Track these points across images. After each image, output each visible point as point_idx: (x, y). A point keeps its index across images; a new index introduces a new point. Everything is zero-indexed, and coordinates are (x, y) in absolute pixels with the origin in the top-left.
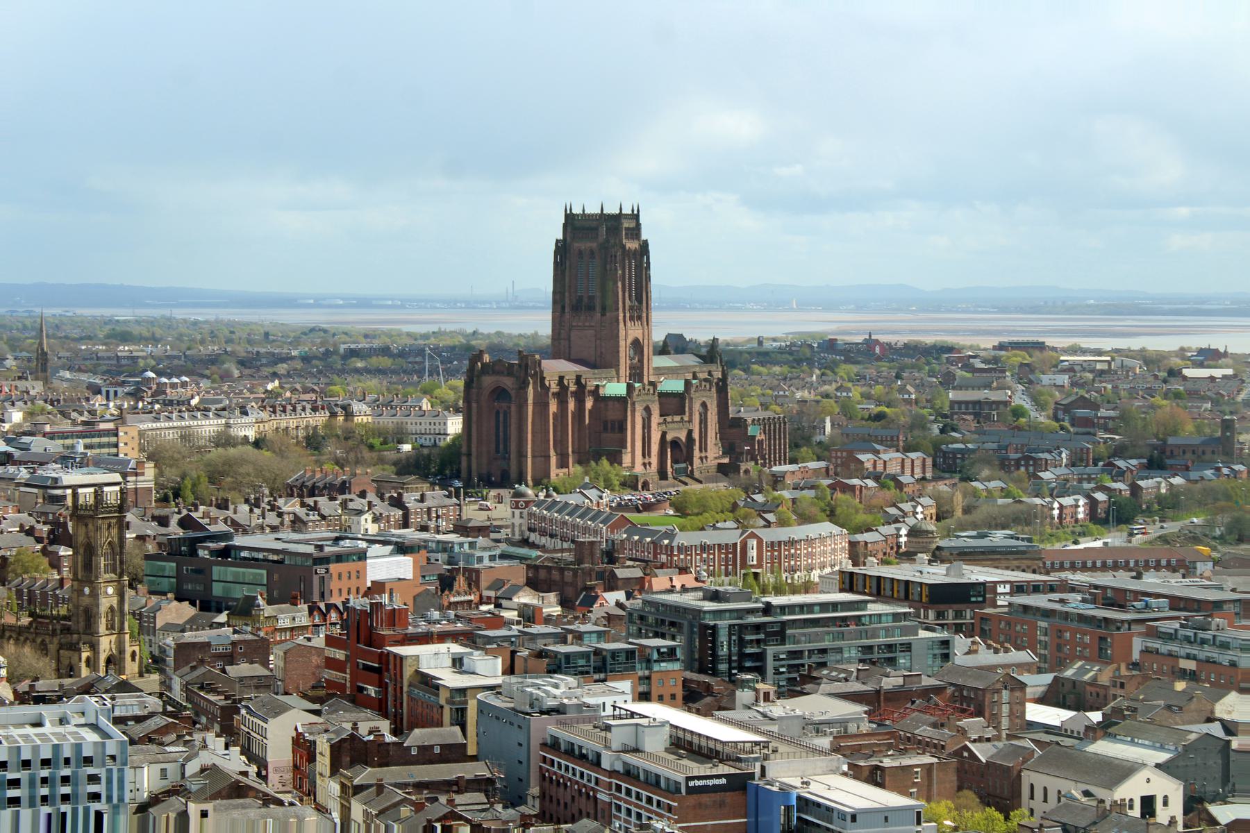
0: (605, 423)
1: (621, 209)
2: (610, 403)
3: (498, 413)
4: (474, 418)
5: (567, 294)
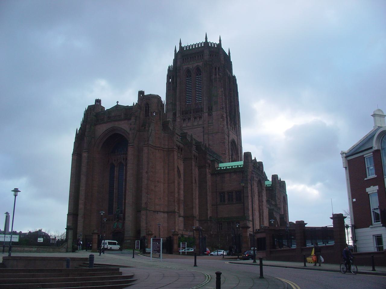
1: (220, 41)
4: (84, 169)
5: (178, 103)
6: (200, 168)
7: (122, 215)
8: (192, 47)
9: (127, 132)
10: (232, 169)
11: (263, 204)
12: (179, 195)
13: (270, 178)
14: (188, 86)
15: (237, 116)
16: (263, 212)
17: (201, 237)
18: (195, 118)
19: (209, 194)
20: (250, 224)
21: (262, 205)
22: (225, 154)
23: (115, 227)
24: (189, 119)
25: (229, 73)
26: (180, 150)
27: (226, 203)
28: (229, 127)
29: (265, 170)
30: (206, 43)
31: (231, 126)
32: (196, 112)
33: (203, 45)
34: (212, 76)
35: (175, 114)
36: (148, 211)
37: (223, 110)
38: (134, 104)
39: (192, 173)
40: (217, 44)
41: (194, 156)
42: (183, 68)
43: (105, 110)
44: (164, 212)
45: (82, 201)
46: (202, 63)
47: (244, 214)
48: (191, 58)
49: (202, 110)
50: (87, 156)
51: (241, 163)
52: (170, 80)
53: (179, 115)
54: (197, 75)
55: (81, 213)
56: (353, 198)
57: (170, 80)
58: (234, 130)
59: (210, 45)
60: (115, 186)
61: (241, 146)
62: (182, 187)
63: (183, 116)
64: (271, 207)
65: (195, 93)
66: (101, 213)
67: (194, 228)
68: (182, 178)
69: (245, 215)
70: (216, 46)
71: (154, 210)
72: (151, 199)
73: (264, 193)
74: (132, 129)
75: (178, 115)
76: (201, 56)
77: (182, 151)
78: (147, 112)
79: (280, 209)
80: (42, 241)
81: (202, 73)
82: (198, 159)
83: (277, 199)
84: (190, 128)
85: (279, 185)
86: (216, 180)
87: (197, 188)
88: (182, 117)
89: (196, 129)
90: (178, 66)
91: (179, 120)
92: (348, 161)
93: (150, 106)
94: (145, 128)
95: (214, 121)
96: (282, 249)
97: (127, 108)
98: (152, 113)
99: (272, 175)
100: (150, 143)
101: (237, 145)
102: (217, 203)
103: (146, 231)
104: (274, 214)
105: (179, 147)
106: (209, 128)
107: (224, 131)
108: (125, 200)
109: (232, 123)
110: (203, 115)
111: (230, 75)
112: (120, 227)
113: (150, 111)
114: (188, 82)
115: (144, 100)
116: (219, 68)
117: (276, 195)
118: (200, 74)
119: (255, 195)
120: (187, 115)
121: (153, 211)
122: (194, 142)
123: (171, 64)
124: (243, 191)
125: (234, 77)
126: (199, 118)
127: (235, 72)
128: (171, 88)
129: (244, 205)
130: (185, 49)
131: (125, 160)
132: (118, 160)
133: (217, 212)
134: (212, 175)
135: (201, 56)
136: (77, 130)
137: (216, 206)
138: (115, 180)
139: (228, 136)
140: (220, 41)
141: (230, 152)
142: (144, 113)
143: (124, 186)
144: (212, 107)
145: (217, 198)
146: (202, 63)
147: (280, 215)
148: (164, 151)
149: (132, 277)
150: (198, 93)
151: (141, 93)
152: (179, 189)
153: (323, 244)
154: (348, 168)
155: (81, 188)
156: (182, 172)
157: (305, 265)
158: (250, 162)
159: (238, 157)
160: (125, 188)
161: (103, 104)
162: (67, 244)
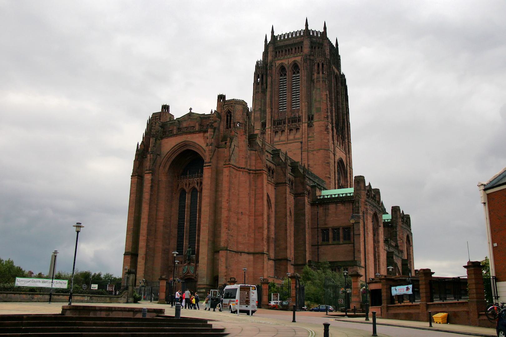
0: (325, 231)
1: (325, 28)
2: (332, 207)
3: (183, 193)
4: (146, 196)
5: (268, 110)
6: (297, 195)
7: (194, 255)
8: (288, 36)
9: (203, 149)
10: (339, 198)
11: (379, 246)
12: (269, 231)
13: (389, 210)
14: (282, 88)
15: (346, 129)
16: (379, 256)
17: (298, 286)
18: (291, 130)
19: (308, 231)
20: (362, 272)
21: (378, 247)
22: (330, 178)
23: (185, 271)
24: (283, 131)
25: (336, 71)
26: (271, 172)
27: (330, 242)
28: (336, 142)
29: (383, 199)
30: (307, 31)
31: (338, 141)
32: (292, 122)
33: (302, 34)
34: (314, 74)
35: (264, 125)
36: (228, 251)
37: (328, 120)
38: (212, 112)
39: (286, 203)
40: (321, 33)
41: (290, 180)
42: (275, 63)
43: (175, 119)
44: (248, 253)
45: (144, 236)
46: (300, 57)
47: (354, 259)
48: (286, 50)
49: (299, 120)
50: (151, 178)
51: (350, 191)
52: (259, 79)
53: (270, 125)
54: (294, 73)
55: (142, 252)
56: (493, 242)
57: (259, 79)
58: (343, 145)
59: (311, 34)
60: (185, 218)
61: (351, 168)
62: (273, 220)
63: (274, 127)
64: (390, 249)
65: (291, 97)
66: (174, 253)
67: (289, 276)
68: (273, 209)
69: (356, 259)
70: (319, 35)
71: (236, 251)
72: (232, 236)
73: (381, 230)
74: (209, 144)
75: (269, 126)
76: (300, 49)
77: (273, 173)
78: (229, 122)
79: (402, 252)
80: (97, 288)
81: (300, 71)
82: (294, 184)
83: (398, 239)
84: (284, 142)
85: (401, 220)
86: (318, 213)
87: (293, 223)
88: (273, 128)
89: (291, 145)
90: (269, 61)
91: (270, 132)
92: (488, 195)
93: (232, 114)
94: (226, 143)
95: (315, 134)
96: (403, 304)
97: (203, 118)
98: (234, 123)
99: (392, 207)
100: (232, 162)
101: (346, 166)
102: (318, 242)
103: (225, 277)
104: (394, 258)
105: (269, 169)
106: (309, 144)
107: (329, 148)
108: (199, 236)
109: (339, 137)
110: (301, 126)
111: (337, 73)
112: (192, 271)
113: (232, 122)
114: (281, 83)
115: (225, 106)
116: (323, 65)
117: (396, 234)
118: (298, 72)
119: (369, 232)
120: (281, 126)
121: (235, 252)
122: (289, 162)
123: (260, 58)
124: (353, 228)
125: (343, 76)
126: (295, 130)
127: (344, 70)
128: (260, 90)
129: (354, 247)
130: (278, 39)
131: (199, 185)
132: (190, 184)
133: (318, 255)
134: (313, 204)
135: (300, 49)
136: (138, 144)
137: (317, 247)
138: (186, 210)
139: (334, 154)
140: (325, 28)
141: (336, 175)
142: (225, 123)
143: (197, 219)
144: (313, 115)
145: (318, 236)
146: (301, 58)
147: (403, 260)
148: (250, 173)
149: (222, 330)
150: (295, 97)
151: (221, 98)
152: (269, 223)
153: (454, 299)
154: (487, 204)
155: (142, 221)
156: (273, 201)
157: (431, 325)
158: (363, 189)
159: (347, 182)
160: (200, 222)
161: (171, 111)
162: (128, 292)
